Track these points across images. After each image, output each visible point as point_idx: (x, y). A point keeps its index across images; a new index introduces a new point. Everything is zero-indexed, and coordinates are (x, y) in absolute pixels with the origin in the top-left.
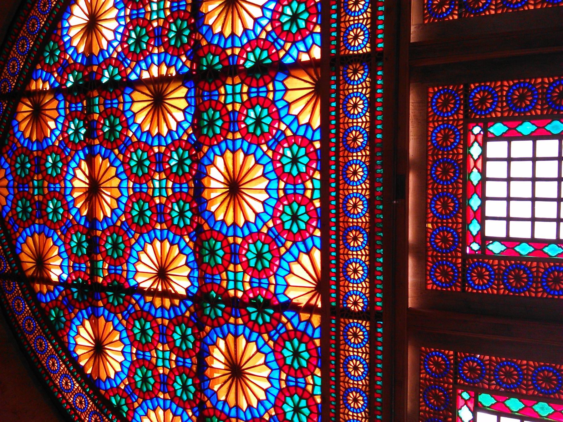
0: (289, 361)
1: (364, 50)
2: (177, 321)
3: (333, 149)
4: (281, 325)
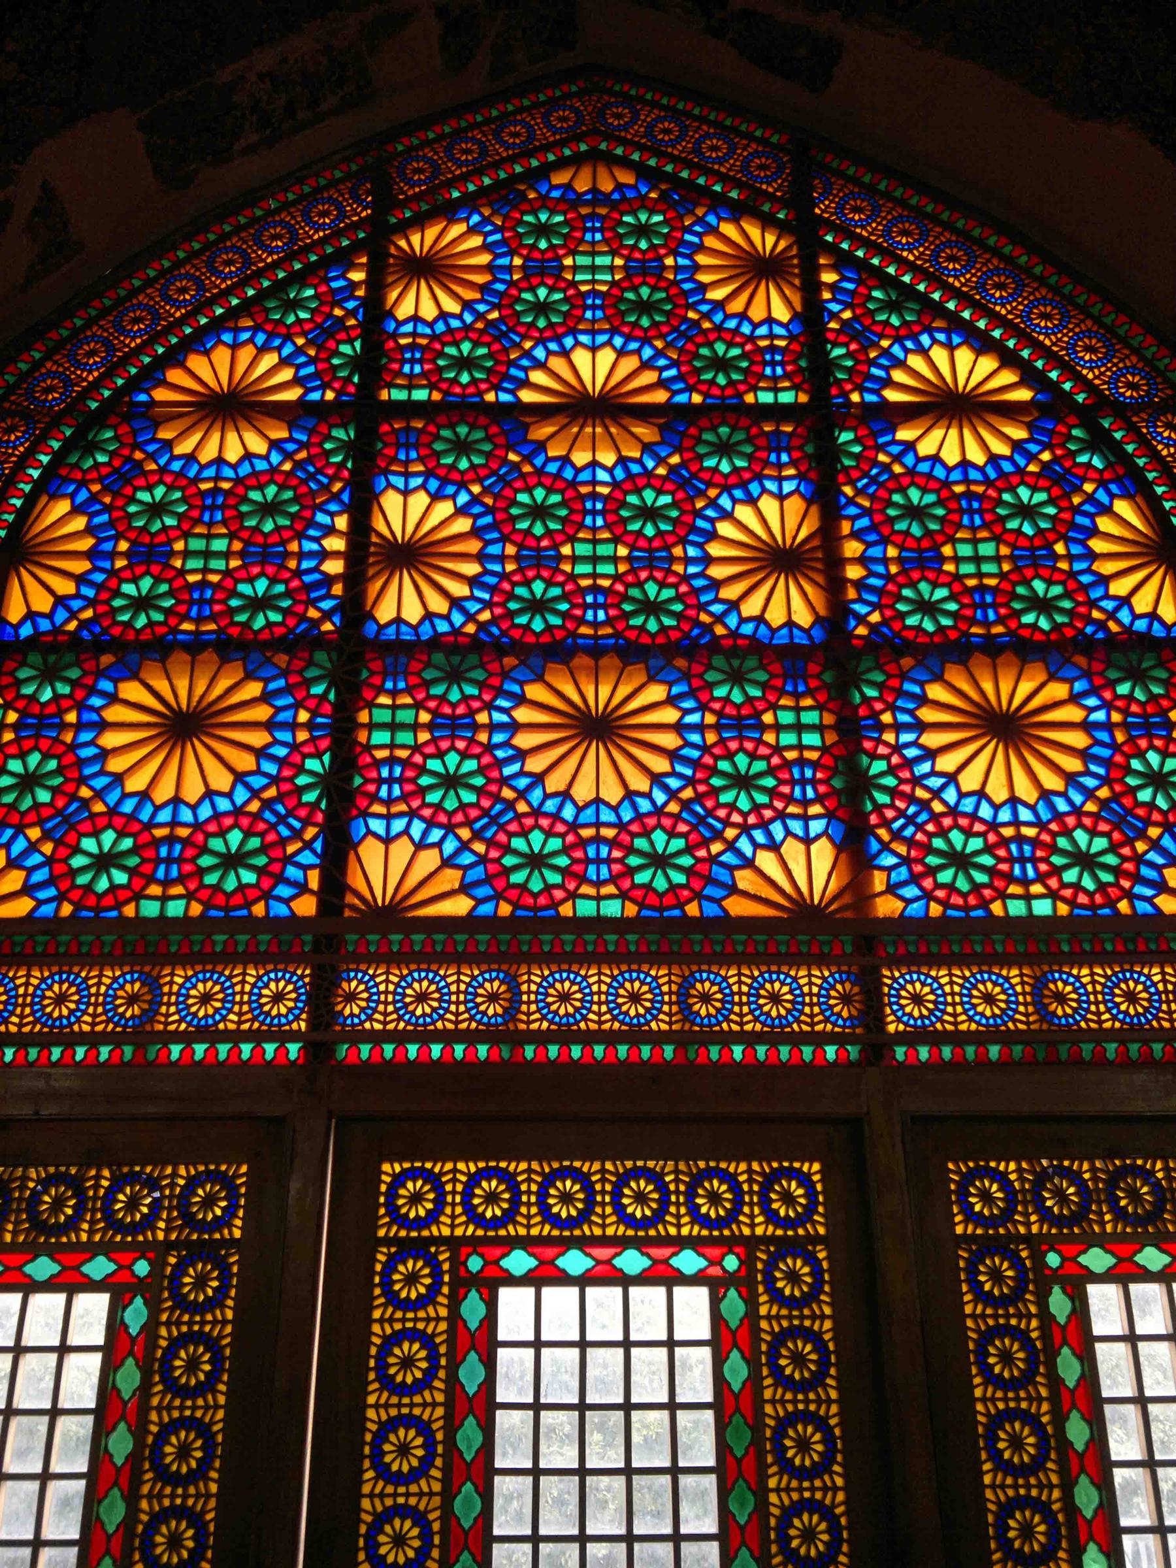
4: (297, 824)
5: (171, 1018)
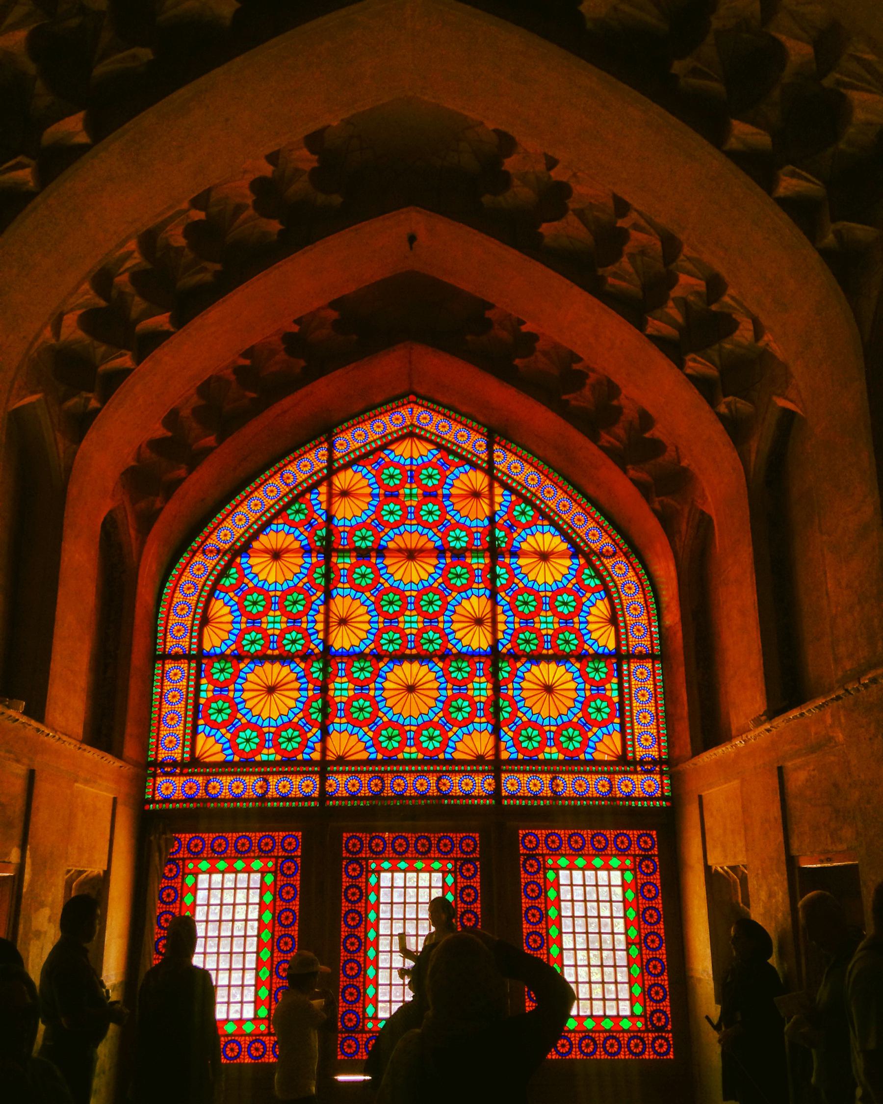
0: (283, 734)
1: (504, 791)
2: (306, 635)
3: (438, 768)
5: (272, 793)
